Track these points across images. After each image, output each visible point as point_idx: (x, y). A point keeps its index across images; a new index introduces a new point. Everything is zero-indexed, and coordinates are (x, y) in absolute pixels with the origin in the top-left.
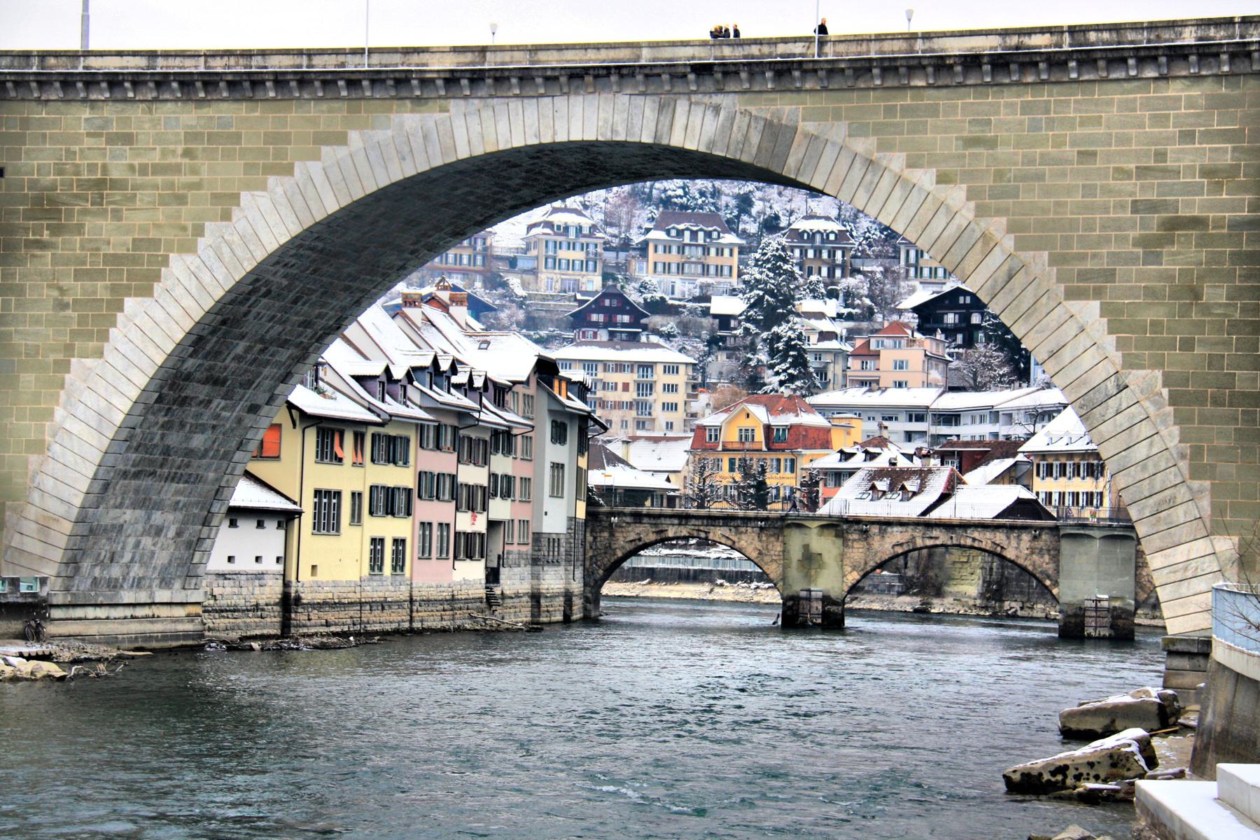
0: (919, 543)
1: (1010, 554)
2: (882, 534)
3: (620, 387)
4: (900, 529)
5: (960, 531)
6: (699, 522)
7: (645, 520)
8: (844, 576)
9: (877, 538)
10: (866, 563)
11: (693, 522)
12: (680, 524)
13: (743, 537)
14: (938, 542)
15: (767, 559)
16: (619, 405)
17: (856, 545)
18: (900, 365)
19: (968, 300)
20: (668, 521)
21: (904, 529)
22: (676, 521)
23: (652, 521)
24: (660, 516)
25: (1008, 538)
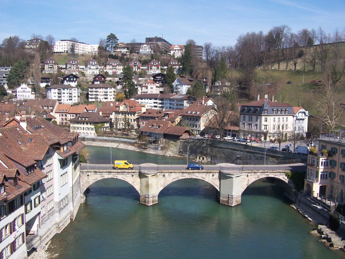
0: (180, 178)
1: (206, 180)
2: (169, 175)
3: (102, 92)
4: (174, 174)
5: (192, 174)
6: (114, 173)
7: (98, 173)
8: (158, 188)
9: (168, 177)
10: (165, 184)
11: (113, 173)
12: (109, 174)
13: (128, 178)
14: (186, 177)
15: (135, 184)
16: (101, 95)
17: (162, 179)
18: (152, 88)
19: (162, 75)
20: (105, 173)
21: (176, 174)
22: (107, 173)
23: (100, 173)
24: (102, 172)
25: (206, 175)
